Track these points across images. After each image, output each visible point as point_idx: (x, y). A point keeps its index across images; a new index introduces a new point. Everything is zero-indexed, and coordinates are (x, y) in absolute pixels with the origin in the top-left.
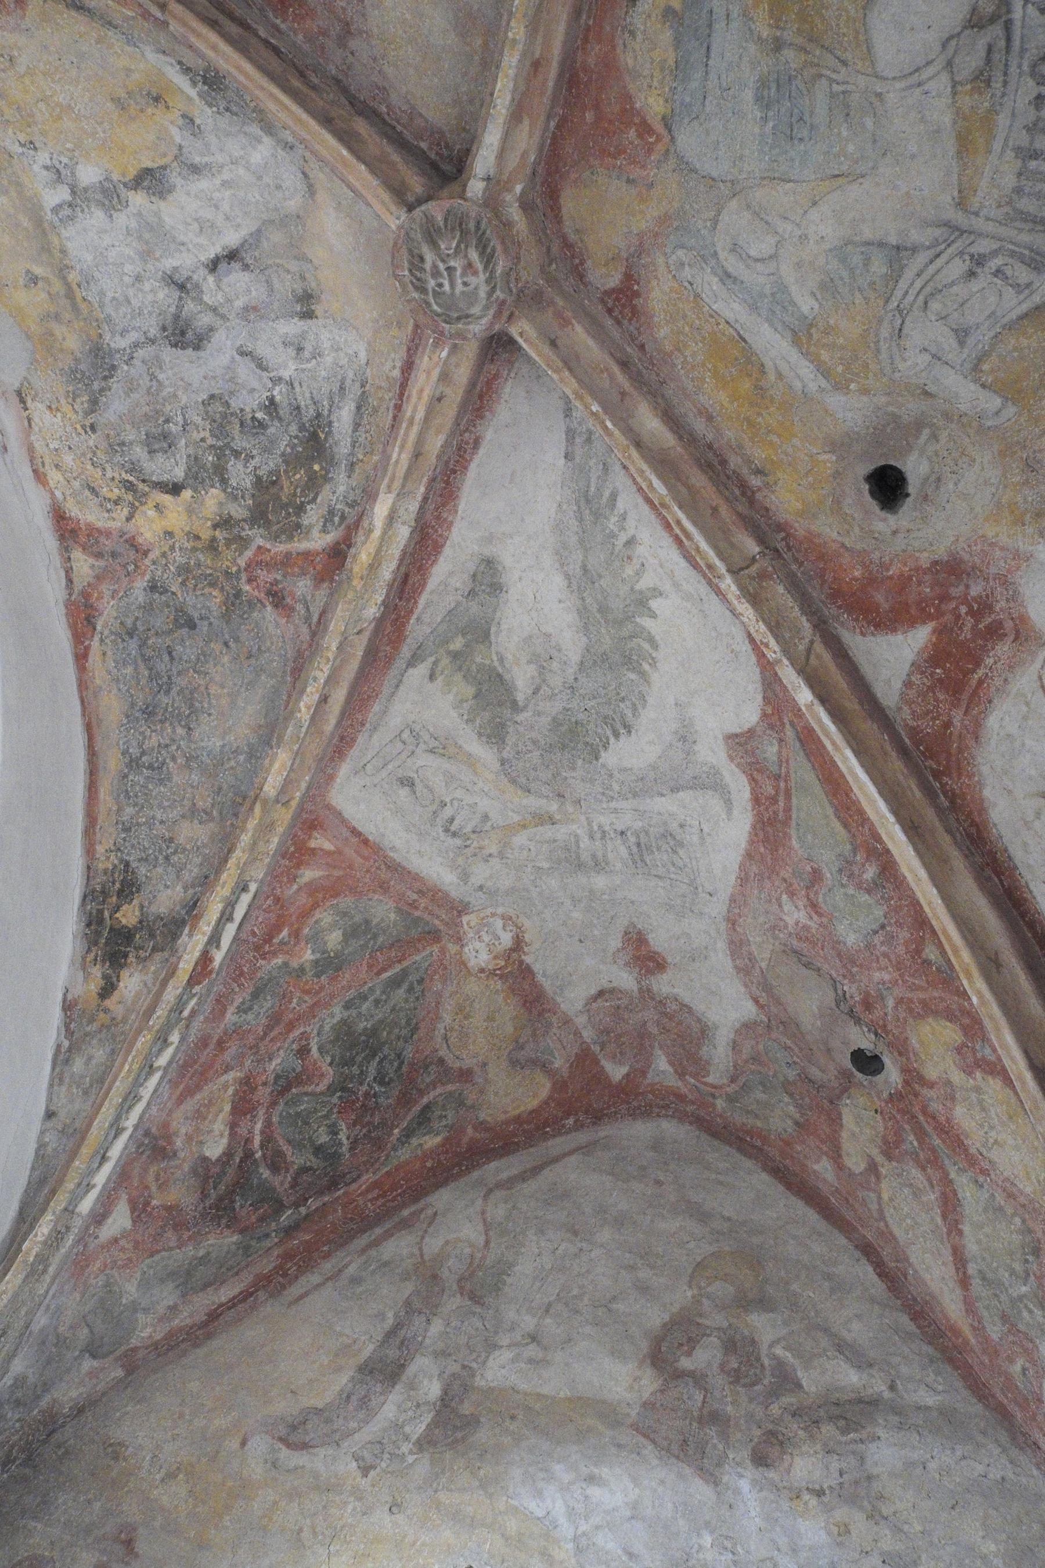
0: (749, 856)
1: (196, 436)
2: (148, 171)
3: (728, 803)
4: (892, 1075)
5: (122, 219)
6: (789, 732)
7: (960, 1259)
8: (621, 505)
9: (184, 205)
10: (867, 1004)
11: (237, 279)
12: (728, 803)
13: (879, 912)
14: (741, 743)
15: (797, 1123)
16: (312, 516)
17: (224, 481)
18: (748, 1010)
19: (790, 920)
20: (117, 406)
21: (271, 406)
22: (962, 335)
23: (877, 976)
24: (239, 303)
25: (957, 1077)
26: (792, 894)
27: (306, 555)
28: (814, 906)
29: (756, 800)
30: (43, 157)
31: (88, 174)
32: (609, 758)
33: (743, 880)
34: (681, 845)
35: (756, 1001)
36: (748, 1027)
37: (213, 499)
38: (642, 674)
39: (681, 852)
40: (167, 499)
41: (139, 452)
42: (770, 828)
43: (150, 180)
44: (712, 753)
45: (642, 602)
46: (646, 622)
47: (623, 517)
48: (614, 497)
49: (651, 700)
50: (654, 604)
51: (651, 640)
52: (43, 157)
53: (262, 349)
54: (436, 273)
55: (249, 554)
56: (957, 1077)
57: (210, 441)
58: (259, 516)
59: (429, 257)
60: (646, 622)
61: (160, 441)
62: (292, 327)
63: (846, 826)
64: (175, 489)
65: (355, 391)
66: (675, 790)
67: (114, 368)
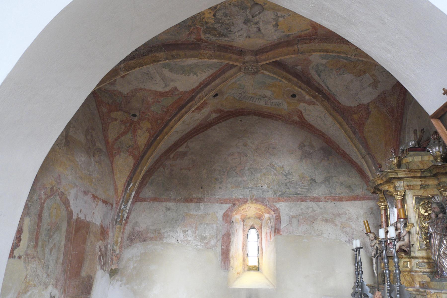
0: (156, 91)
1: (226, 21)
2: (278, 26)
3: (164, 88)
4: (135, 119)
5: (271, 20)
6: (181, 96)
7: (118, 138)
8: (211, 70)
9: (270, 27)
10: (143, 113)
11: (255, 30)
12: (164, 88)
13: (159, 112)
14: (176, 89)
15: (108, 103)
16: (207, 35)
17: (216, 23)
18: (125, 93)
19: (148, 99)
20: (234, 9)
21: (231, 31)
22: (233, 94)
23: (149, 113)
24: (251, 29)
25: (144, 129)
26: (153, 99)
27: (200, 35)
28: (154, 102)
29: (167, 92)
30: (287, 16)
31: (281, 19)
32: (164, 69)
33: (151, 91)
34: (152, 80)
35: (128, 94)
36: (120, 93)
37: (212, 21)
38: (182, 74)
39: (150, 80)
40: (212, 14)
41: (223, 11)
42: (162, 94)
43: (277, 25)
44: (172, 85)
45: (195, 74)
46: (192, 74)
47: (209, 71)
48: (211, 69)
49: (178, 75)
50: (195, 75)
51: (188, 75)
52: (287, 16)
53: (242, 31)
54: (252, 68)
55: (200, 27)
56: (144, 129)
57: (225, 22)
58: (208, 28)
59: (254, 67)
60: (192, 74)
61: (225, 15)
62: (245, 35)
63: (170, 105)
64: (214, 15)
65: (232, 41)
66: (162, 79)
67: (243, 10)
